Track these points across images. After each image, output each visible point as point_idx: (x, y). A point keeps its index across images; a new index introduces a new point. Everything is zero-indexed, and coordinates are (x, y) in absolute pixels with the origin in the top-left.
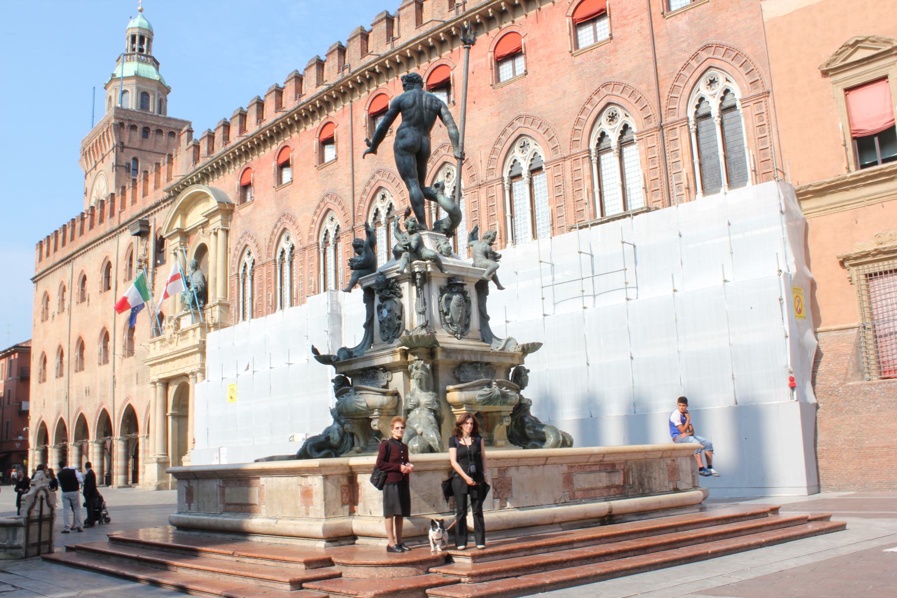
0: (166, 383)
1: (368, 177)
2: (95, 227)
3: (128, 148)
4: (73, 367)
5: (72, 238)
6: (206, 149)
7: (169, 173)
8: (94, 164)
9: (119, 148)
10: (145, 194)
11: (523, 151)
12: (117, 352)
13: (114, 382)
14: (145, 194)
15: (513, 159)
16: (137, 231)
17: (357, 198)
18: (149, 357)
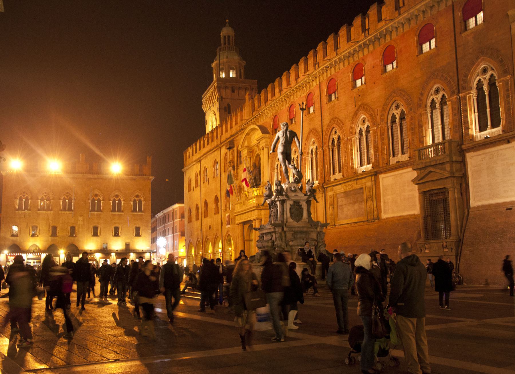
0: (244, 223)
1: (328, 122)
2: (210, 144)
3: (225, 99)
4: (203, 215)
5: (200, 150)
6: (257, 104)
7: (242, 116)
8: (209, 108)
9: (220, 99)
10: (231, 128)
11: (397, 109)
12: (222, 208)
13: (222, 223)
14: (231, 128)
15: (392, 113)
16: (228, 147)
17: (324, 133)
18: (235, 212)
